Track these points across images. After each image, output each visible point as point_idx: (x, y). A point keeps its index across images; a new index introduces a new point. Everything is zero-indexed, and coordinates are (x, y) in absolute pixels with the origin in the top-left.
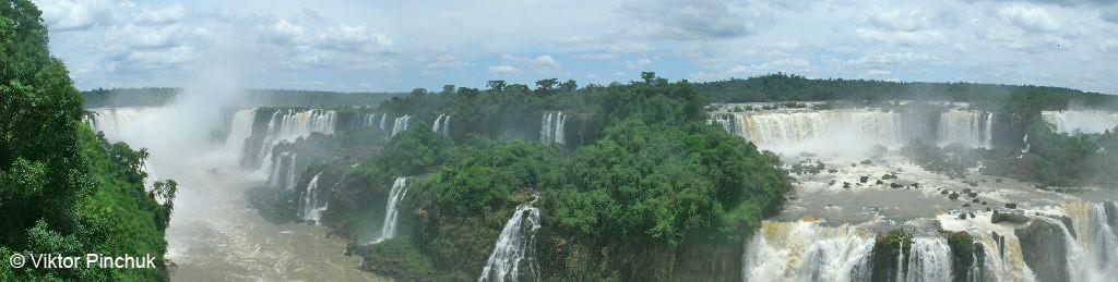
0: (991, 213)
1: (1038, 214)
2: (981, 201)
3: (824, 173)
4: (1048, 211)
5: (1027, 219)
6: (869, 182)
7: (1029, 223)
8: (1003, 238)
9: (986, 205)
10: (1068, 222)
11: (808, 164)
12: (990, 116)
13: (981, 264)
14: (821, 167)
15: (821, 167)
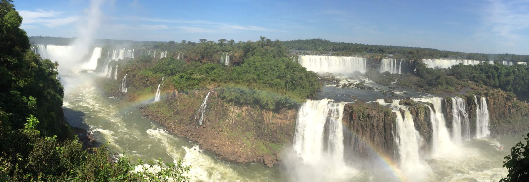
0: (399, 100)
1: (419, 102)
4: (424, 100)
6: (352, 86)
9: (397, 97)
10: (432, 106)
15: (333, 79)
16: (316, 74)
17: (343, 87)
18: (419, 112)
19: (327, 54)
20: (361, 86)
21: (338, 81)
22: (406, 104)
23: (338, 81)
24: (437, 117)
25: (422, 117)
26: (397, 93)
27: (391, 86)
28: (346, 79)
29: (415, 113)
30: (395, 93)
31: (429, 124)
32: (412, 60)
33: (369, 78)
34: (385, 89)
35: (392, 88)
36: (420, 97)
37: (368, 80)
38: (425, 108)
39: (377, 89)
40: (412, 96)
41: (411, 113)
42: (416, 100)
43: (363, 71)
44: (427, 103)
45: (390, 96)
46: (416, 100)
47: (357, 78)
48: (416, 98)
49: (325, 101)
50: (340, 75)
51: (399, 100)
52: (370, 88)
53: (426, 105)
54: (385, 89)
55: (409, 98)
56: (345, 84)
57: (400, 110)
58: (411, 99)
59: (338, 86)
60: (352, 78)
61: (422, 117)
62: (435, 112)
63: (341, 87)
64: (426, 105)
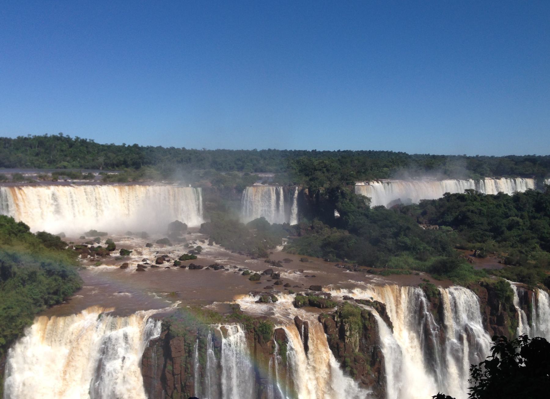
0: (294, 296)
1: (346, 298)
2: (284, 284)
3: (116, 254)
4: (358, 294)
5: (334, 304)
6: (166, 264)
7: (336, 309)
8: (306, 324)
9: (288, 287)
10: (382, 309)
11: (96, 245)
12: (297, 188)
13: (283, 351)
14: (112, 247)
15: (112, 247)
16: (57, 238)
17: (140, 268)
18: (347, 327)
19: (89, 180)
20: (190, 261)
21: (125, 252)
22: (312, 304)
23: (125, 252)
24: (399, 341)
25: (354, 338)
26: (286, 275)
27: (272, 258)
28: (148, 245)
29: (335, 331)
30: (283, 275)
31: (376, 359)
32: (324, 185)
33: (213, 239)
34: (256, 267)
35: (274, 264)
36: (350, 288)
37: (210, 244)
38: (363, 316)
39: (235, 267)
40: (327, 282)
41: (326, 329)
42: (338, 294)
43: (194, 220)
44: (367, 302)
45: (270, 284)
46: (338, 294)
47: (179, 241)
48: (338, 288)
49: (88, 318)
50: (130, 234)
51: (294, 296)
52: (216, 267)
53: (368, 308)
54: (256, 267)
55: (319, 288)
56: (144, 260)
57: (298, 323)
58: (325, 290)
59: (125, 266)
60: (162, 242)
61: (354, 338)
62: (390, 325)
63: (133, 267)
64: (368, 308)
